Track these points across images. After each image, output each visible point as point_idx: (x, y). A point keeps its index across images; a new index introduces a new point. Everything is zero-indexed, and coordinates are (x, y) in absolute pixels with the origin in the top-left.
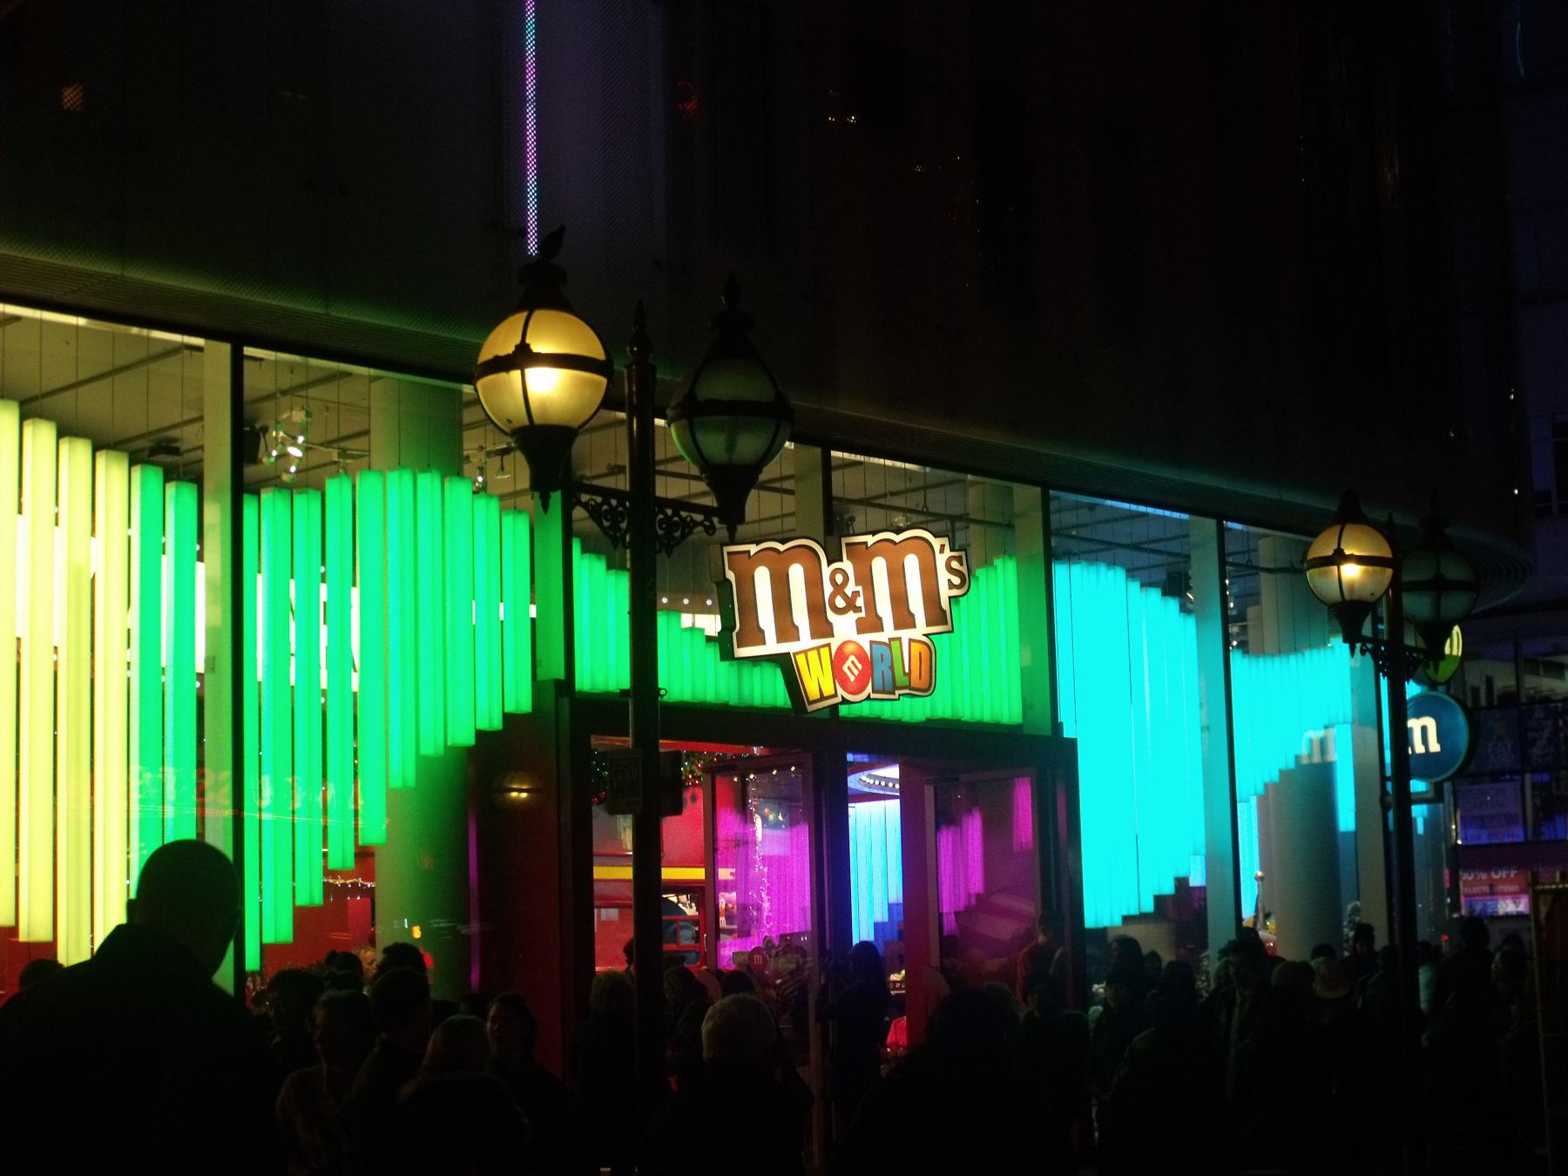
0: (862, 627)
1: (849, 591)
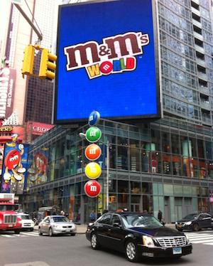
0: (110, 57)
1: (106, 50)
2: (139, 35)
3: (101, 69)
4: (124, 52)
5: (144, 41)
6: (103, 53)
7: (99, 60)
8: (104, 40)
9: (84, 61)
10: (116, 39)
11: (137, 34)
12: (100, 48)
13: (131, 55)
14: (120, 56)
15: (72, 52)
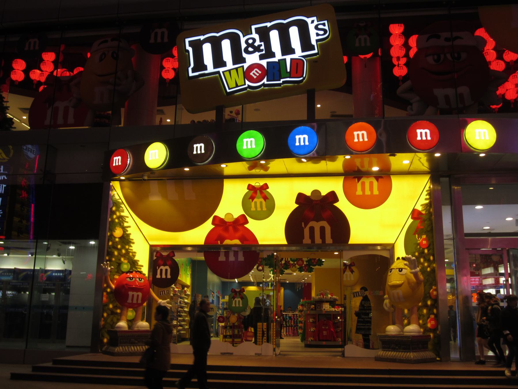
0: (262, 57)
1: (256, 44)
2: (312, 23)
4: (287, 49)
5: (321, 32)
7: (244, 61)
8: (253, 27)
9: (218, 61)
10: (273, 27)
11: (309, 20)
12: (247, 42)
13: (298, 53)
15: (197, 47)
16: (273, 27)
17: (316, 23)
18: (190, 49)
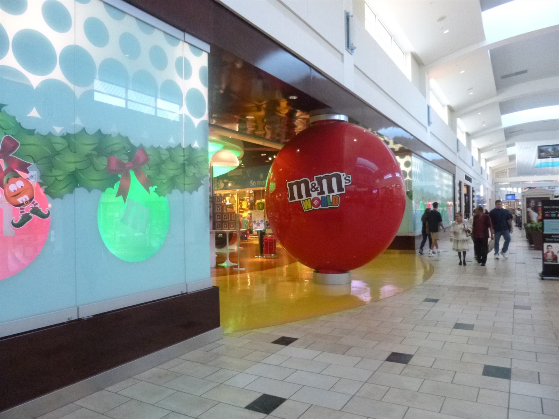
0: (319, 194)
1: (316, 187)
2: (343, 175)
3: (312, 204)
4: (331, 190)
5: (347, 182)
6: (313, 189)
7: (310, 195)
10: (324, 178)
11: (342, 174)
13: (336, 192)
14: (327, 193)
15: (291, 186)
16: (324, 178)
17: (345, 176)
18: (288, 188)
